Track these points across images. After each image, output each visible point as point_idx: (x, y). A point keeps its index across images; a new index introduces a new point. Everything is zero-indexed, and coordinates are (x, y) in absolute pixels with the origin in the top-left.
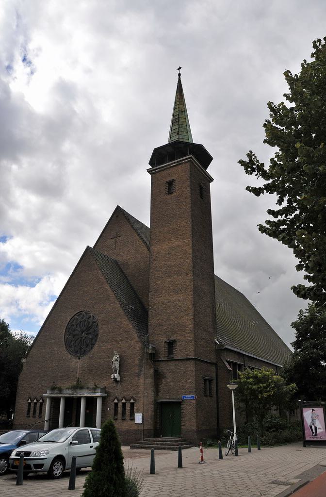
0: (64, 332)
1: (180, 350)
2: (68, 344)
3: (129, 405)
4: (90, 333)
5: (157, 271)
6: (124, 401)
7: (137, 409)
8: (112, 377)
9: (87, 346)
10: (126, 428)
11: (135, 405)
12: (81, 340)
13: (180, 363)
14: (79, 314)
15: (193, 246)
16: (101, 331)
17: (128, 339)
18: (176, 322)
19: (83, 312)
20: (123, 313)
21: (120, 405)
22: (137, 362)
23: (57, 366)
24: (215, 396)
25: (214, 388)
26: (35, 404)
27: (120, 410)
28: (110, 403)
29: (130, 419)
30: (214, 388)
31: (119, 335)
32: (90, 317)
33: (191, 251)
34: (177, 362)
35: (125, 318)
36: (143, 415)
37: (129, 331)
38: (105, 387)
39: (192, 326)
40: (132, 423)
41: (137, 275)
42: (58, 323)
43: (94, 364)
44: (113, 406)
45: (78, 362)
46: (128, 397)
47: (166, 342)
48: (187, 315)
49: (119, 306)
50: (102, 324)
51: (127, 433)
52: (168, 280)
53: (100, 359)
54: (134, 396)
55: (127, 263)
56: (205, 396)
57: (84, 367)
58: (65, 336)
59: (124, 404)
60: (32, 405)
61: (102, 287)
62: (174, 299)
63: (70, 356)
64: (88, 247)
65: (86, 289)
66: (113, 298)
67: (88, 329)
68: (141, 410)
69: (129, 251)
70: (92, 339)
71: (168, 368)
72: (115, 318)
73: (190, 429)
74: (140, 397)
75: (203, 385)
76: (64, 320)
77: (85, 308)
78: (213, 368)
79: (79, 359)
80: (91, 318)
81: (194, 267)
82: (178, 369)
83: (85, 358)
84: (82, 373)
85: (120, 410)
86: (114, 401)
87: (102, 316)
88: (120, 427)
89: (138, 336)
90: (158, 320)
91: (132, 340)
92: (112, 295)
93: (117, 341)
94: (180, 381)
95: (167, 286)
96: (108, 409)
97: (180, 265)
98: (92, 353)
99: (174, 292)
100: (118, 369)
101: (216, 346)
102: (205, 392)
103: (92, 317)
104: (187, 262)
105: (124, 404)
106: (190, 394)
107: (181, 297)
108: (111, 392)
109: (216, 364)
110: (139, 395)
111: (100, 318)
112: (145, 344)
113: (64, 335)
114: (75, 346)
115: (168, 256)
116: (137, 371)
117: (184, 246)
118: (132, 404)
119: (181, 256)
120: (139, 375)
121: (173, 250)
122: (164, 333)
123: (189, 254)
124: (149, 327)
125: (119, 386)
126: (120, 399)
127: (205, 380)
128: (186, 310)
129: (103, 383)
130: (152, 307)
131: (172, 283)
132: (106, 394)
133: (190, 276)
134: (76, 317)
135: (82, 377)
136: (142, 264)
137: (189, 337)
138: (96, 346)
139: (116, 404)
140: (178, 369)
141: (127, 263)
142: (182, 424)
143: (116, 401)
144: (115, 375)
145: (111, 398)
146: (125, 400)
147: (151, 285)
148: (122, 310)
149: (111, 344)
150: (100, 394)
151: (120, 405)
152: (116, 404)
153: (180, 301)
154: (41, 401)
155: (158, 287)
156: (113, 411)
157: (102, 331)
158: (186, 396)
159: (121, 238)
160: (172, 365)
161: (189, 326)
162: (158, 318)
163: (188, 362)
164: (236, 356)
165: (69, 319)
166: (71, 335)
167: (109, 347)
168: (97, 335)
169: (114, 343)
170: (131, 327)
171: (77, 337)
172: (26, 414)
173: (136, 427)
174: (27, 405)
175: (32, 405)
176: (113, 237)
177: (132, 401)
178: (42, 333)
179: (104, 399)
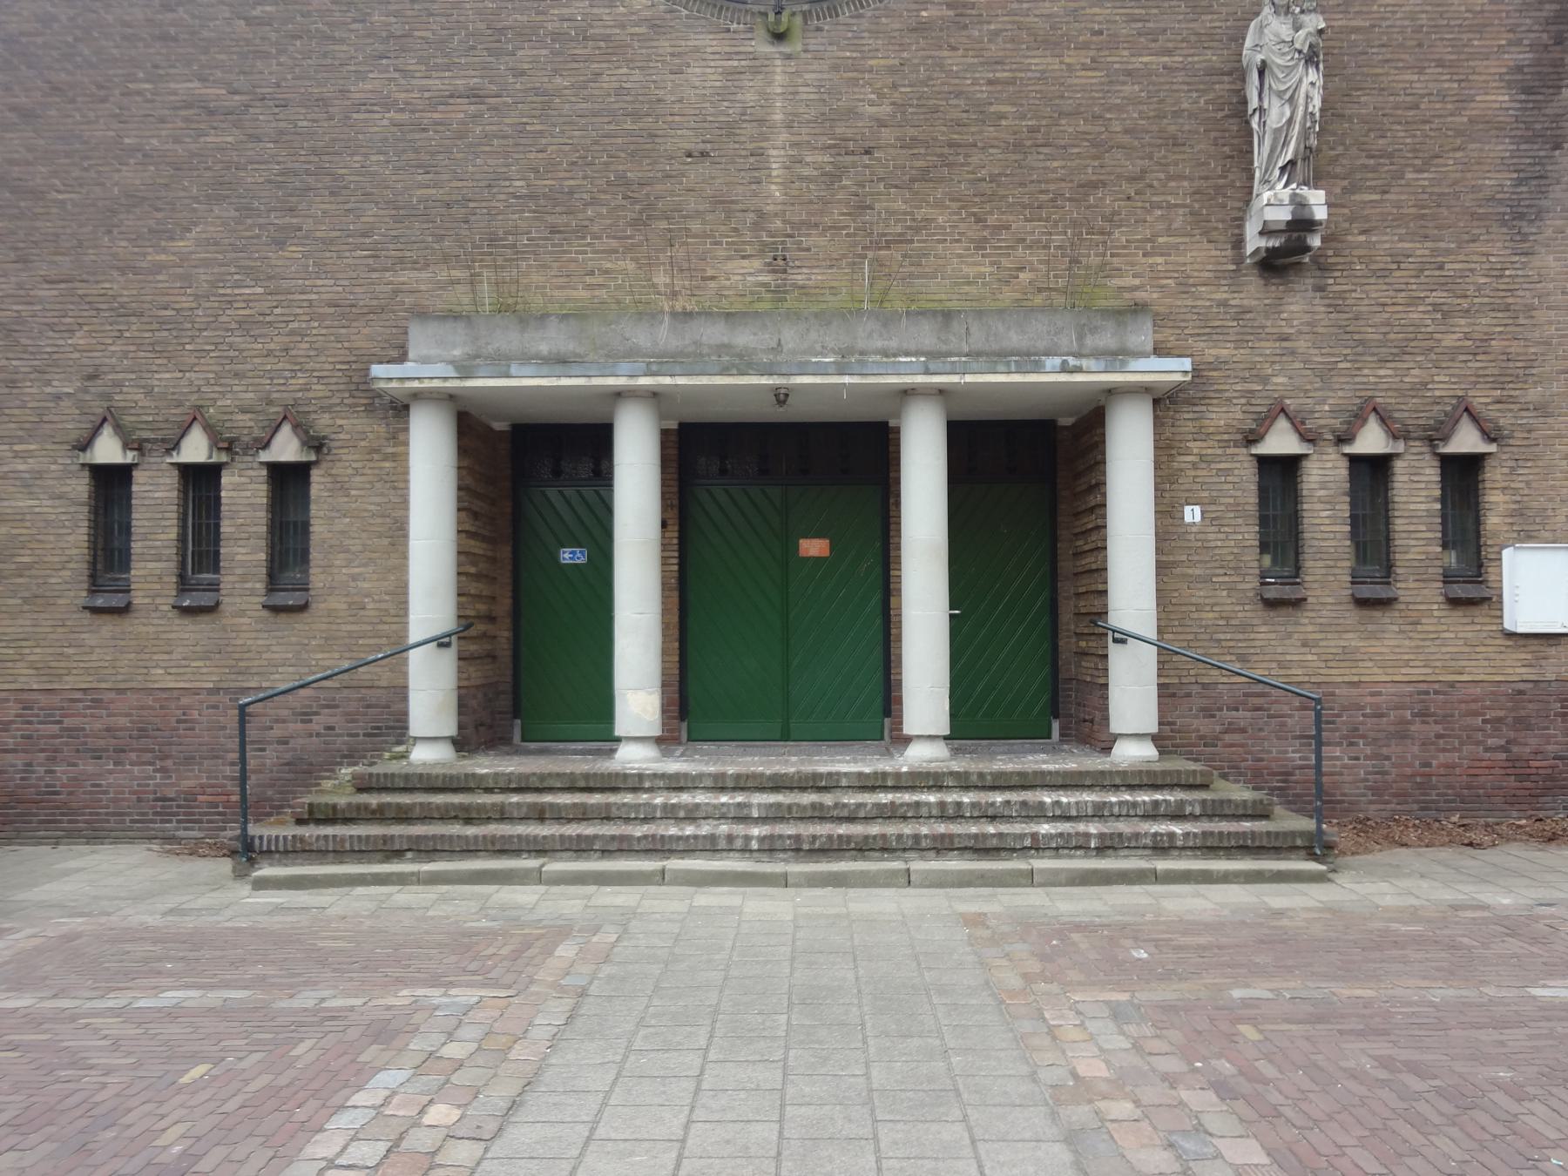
10: (1417, 673)
11: (1493, 475)
22: (1498, 100)
23: (474, 95)
40: (1468, 632)
43: (983, 90)
45: (759, 67)
46: (1408, 411)
51: (1423, 715)
53: (1051, 43)
54: (1480, 399)
57: (851, 113)
84: (832, 177)
88: (1338, 674)
108: (1218, 364)
110: (1534, 394)
116: (1496, 181)
126: (1325, 417)
135: (836, 214)
145: (1223, 416)
173: (1516, 667)
174: (81, 487)
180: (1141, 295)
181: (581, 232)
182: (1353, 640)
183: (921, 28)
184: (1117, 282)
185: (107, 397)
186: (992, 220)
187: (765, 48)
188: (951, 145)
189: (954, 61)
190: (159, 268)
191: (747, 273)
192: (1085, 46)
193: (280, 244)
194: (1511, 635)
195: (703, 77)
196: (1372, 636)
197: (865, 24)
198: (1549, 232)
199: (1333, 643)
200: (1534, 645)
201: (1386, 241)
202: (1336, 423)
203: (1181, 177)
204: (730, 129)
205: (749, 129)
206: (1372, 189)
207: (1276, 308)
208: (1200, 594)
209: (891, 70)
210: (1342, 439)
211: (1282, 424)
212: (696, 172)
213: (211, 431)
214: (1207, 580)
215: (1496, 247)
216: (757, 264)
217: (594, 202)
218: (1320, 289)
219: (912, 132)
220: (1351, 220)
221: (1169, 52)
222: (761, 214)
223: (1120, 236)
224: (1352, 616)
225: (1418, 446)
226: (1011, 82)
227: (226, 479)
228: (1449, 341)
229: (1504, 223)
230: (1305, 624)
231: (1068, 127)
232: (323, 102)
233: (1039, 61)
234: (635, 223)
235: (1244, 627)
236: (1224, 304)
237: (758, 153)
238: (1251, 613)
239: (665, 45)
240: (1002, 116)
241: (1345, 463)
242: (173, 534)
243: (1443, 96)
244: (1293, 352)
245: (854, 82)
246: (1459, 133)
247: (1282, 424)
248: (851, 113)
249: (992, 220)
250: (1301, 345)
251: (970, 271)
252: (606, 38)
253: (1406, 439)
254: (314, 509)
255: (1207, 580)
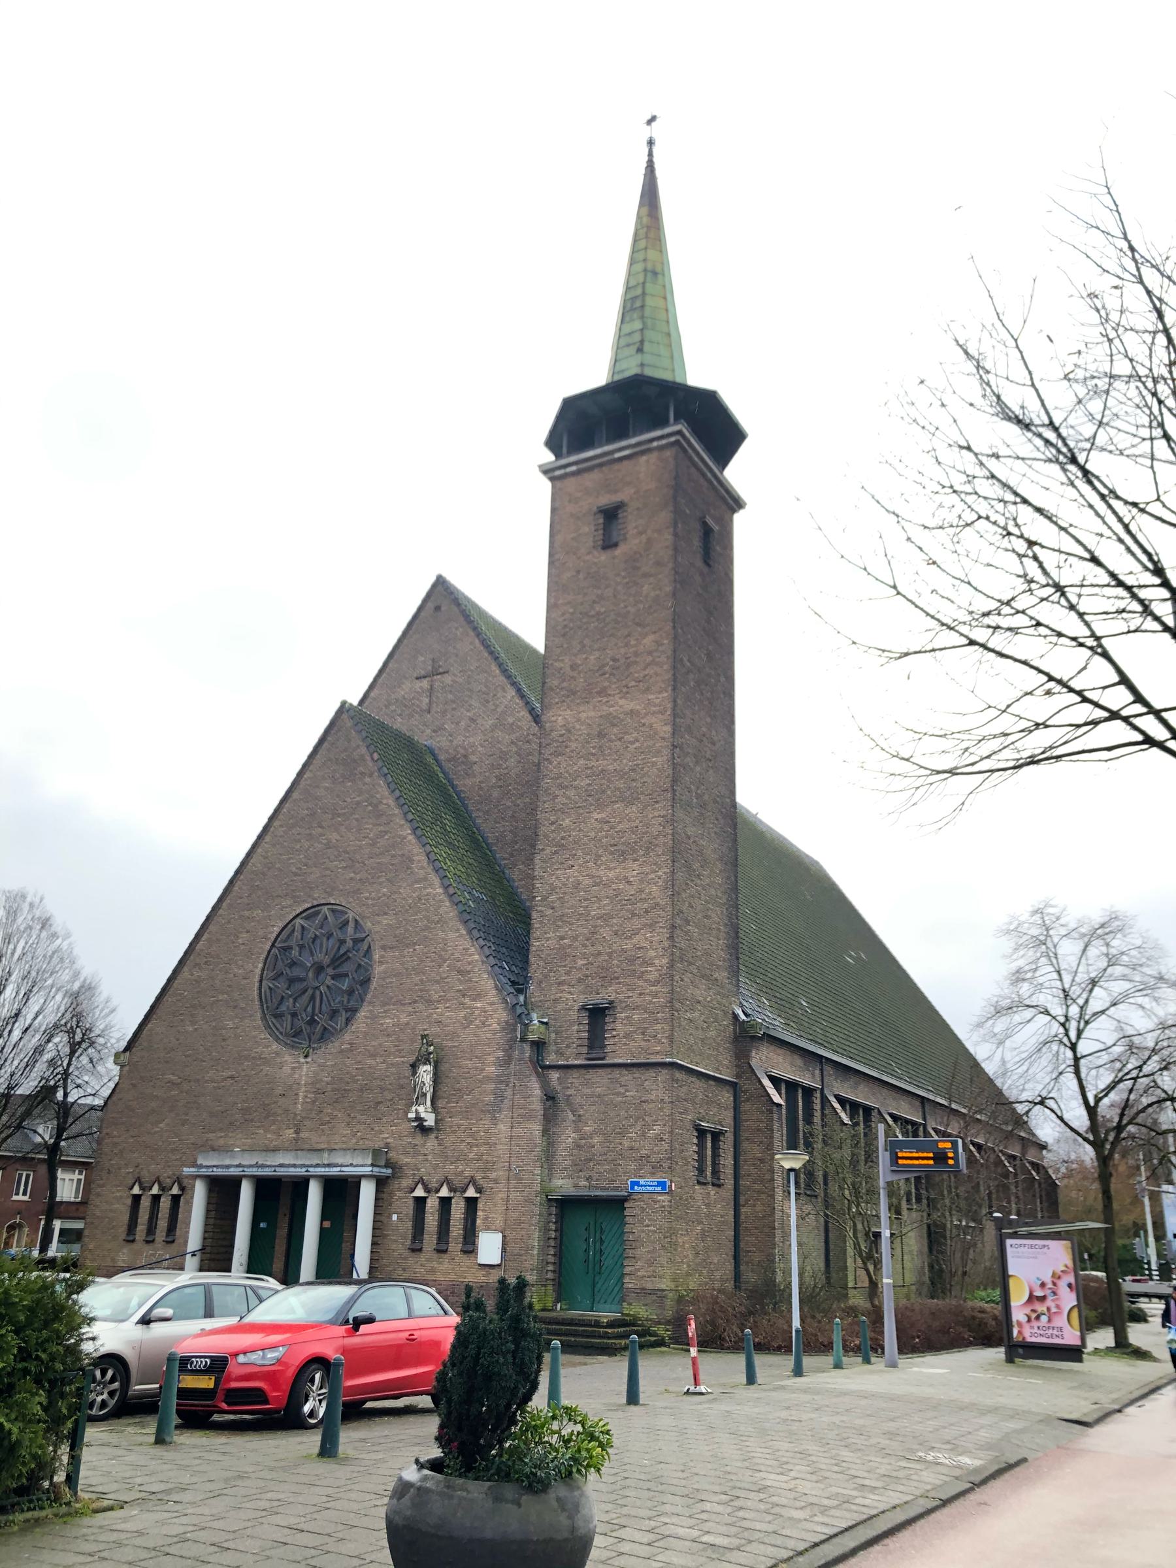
0: (258, 971)
1: (627, 1036)
2: (272, 1011)
3: (462, 1204)
4: (346, 975)
5: (561, 786)
6: (444, 1192)
7: (486, 1219)
8: (412, 1115)
9: (334, 1013)
10: (452, 1277)
11: (480, 1205)
12: (313, 998)
13: (626, 1077)
14: (311, 913)
15: (675, 715)
16: (378, 970)
17: (464, 996)
18: (615, 947)
19: (325, 908)
20: (451, 914)
21: (432, 1204)
22: (491, 1070)
23: (232, 1077)
24: (729, 1183)
25: (727, 1161)
26: (156, 1199)
27: (431, 1220)
28: (400, 1198)
29: (461, 1251)
30: (727, 1161)
31: (438, 982)
32: (346, 923)
33: (668, 728)
34: (617, 1073)
35: (458, 930)
36: (504, 1237)
37: (469, 972)
38: (387, 1145)
39: (665, 961)
41: (496, 794)
42: (240, 941)
44: (409, 1208)
46: (458, 1182)
47: (583, 1008)
48: (652, 926)
49: (441, 890)
50: (384, 948)
52: (596, 815)
53: (373, 1056)
54: (478, 1176)
55: (465, 756)
56: (699, 1183)
58: (261, 981)
59: (445, 1203)
60: (145, 1203)
61: (386, 832)
62: (611, 875)
63: (275, 1046)
64: (344, 703)
65: (334, 837)
66: (422, 868)
67: (339, 960)
68: (499, 1222)
69: (472, 720)
70: (350, 992)
71: (587, 1091)
72: (427, 928)
73: (649, 1286)
74: (496, 1181)
75: (695, 1148)
76: (261, 933)
77: (330, 895)
78: (726, 1097)
79: (306, 1056)
80: (350, 929)
81: (674, 781)
82: (618, 1094)
83: (328, 1055)
84: (314, 1102)
85: (431, 1220)
86: (413, 1190)
87: (386, 920)
89: (496, 987)
90: (562, 938)
91: (478, 997)
92: (420, 857)
93: (429, 1002)
94: (623, 1134)
95: (592, 834)
96: (395, 1217)
97: (633, 770)
98: (347, 1037)
99: (612, 853)
100: (428, 1089)
101: (734, 1025)
102: (701, 1170)
103: (351, 924)
104: (654, 764)
105: (445, 1203)
106: (653, 1174)
107: (633, 870)
108: (407, 1164)
109: (733, 1085)
110: (493, 1175)
111: (377, 928)
112: (519, 1016)
113: (257, 978)
114: (294, 1015)
115: (595, 742)
116: (489, 1098)
117: (646, 714)
118: (472, 1203)
119: (637, 744)
120: (493, 1111)
121: (614, 725)
122: (579, 981)
123: (663, 738)
124: (532, 959)
125: (431, 1143)
126: (433, 1185)
127: (701, 1133)
128: (646, 912)
129: (381, 1132)
130: (544, 899)
131: (606, 827)
132: (390, 1171)
133: (661, 809)
134: (298, 921)
135: (313, 1115)
136: (512, 762)
137: (655, 995)
138: (362, 1014)
139: (420, 1202)
140: (618, 1094)
141: (465, 756)
142: (627, 1270)
143: (420, 1192)
144: (421, 1109)
145: (406, 1183)
146: (451, 1190)
147: (542, 830)
148: (448, 904)
149: (410, 1009)
150: (370, 1169)
151: (432, 1204)
152: (420, 1202)
153: (629, 883)
154: (175, 1190)
155: (563, 839)
156: (410, 1224)
157: (383, 967)
158: (642, 1182)
159: (448, 679)
160: (600, 1078)
161: (657, 962)
162: (560, 933)
163: (651, 1073)
164: (799, 1061)
165: (276, 930)
166: (282, 979)
167: (404, 1019)
168: (366, 982)
169: (420, 1006)
170: (477, 957)
171: (298, 986)
172: (122, 1231)
175: (145, 1203)
176: (423, 673)
177: (471, 1193)
178: (185, 973)
179: (381, 1183)
180: (388, 1140)
181: (252, 1121)
182: (435, 1265)
183: (342, 1051)
184: (382, 1136)
185: (139, 1173)
186: (352, 1115)
187: (302, 1060)
188: (345, 1090)
189: (348, 1062)
190: (156, 1132)
191: (290, 1133)
192: (381, 1056)
193: (183, 1125)
194: (480, 1265)
195: (287, 1069)
196: (440, 1263)
197: (327, 1051)
198: (502, 1116)
199: (429, 1265)
200: (487, 1269)
201: (456, 1120)
202: (436, 1185)
203: (402, 1099)
204: (290, 1086)
205: (295, 1086)
206: (453, 1102)
207: (424, 1145)
208: (394, 1246)
209: (332, 1065)
210: (438, 1191)
211: (420, 1186)
212: (282, 1101)
213: (160, 1185)
214: (396, 1241)
215: (487, 1123)
216: (292, 1130)
217: (256, 1111)
218: (437, 1138)
219: (335, 1086)
220: (447, 1113)
221: (403, 1057)
222: (296, 1115)
223: (384, 1120)
224: (435, 1255)
225: (458, 1194)
226: (362, 1068)
227: (162, 1200)
228: (471, 1156)
229: (490, 1113)
230: (422, 1258)
231: (376, 1083)
232: (198, 1080)
233: (370, 1062)
234: (265, 1118)
235: (405, 1259)
236: (410, 1143)
237: (297, 1094)
238: (407, 1253)
239: (279, 1060)
240: (358, 1080)
241: (438, 1200)
242: (147, 1217)
243: (476, 1068)
244: (427, 1160)
245: (322, 1070)
246: (480, 1081)
247: (420, 1186)
248: (321, 1080)
249: (352, 1115)
250: (430, 1157)
251: (345, 1132)
252: (265, 1058)
253: (455, 1192)
254: (180, 1210)
255: (396, 1241)
